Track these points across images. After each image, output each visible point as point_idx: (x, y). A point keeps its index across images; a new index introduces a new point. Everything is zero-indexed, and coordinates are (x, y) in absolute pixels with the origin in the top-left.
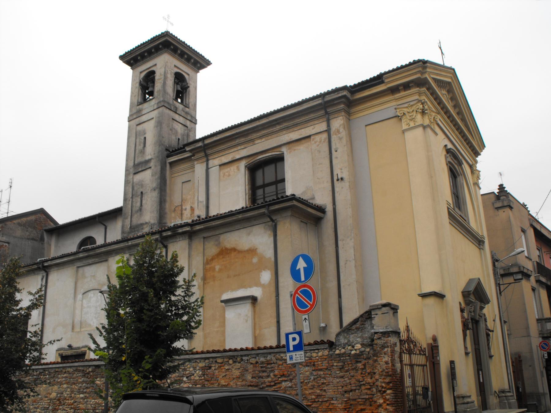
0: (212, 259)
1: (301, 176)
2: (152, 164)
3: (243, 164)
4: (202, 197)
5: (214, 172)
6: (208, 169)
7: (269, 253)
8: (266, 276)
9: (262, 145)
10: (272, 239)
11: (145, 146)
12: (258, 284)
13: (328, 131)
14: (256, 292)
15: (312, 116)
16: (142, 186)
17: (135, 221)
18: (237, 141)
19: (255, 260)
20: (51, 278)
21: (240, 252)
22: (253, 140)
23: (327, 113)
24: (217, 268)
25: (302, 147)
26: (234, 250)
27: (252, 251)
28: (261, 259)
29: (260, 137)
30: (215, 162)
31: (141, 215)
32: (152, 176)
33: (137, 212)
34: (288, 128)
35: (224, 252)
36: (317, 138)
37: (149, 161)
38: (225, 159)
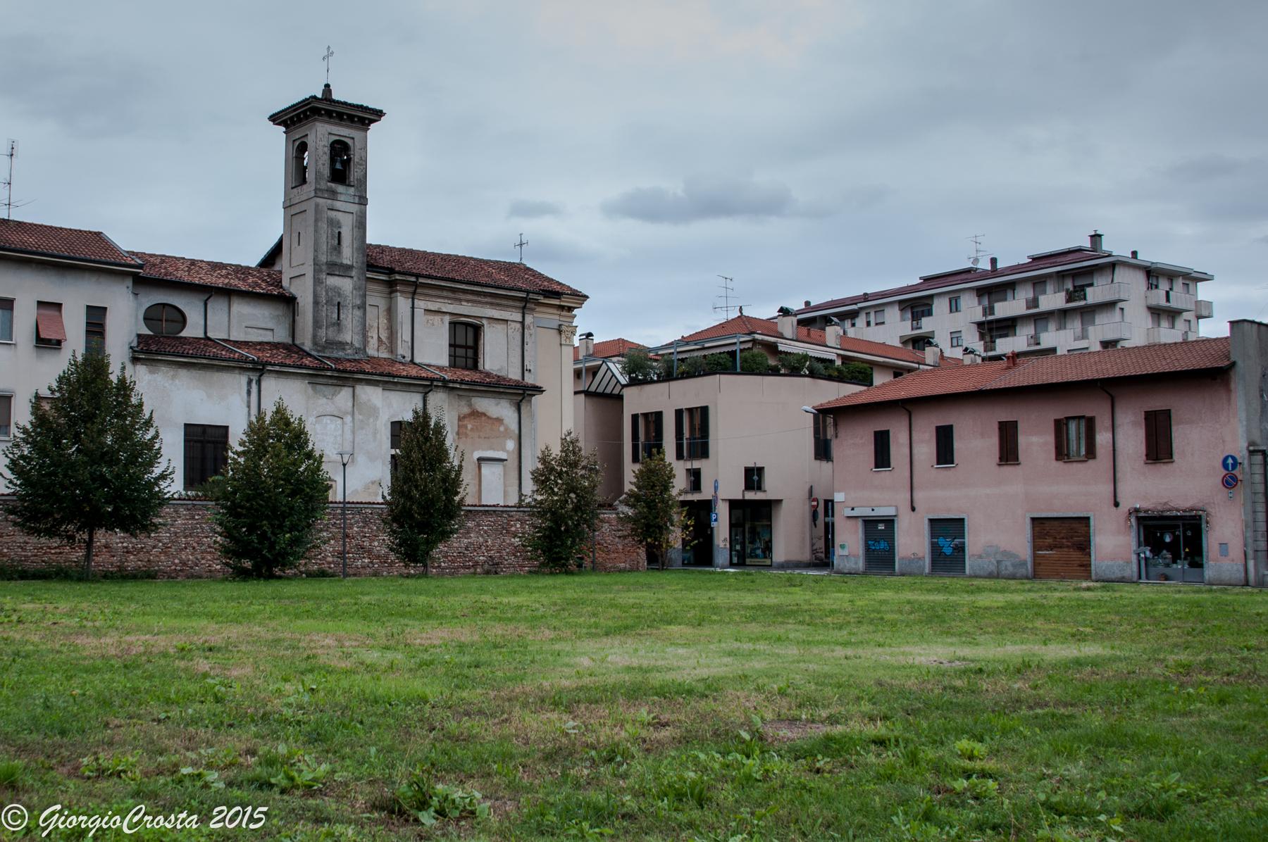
0: (464, 417)
1: (497, 355)
2: (353, 274)
3: (447, 319)
4: (407, 337)
5: (419, 313)
6: (413, 308)
7: (514, 427)
8: (511, 445)
9: (468, 309)
10: (516, 415)
11: (339, 243)
12: (504, 449)
13: (523, 323)
14: (502, 455)
15: (511, 303)
16: (339, 295)
17: (332, 333)
18: (445, 294)
19: (502, 429)
20: (263, 384)
21: (489, 418)
22: (460, 300)
23: (524, 308)
24: (469, 427)
25: (500, 327)
26: (484, 414)
27: (499, 420)
28: (507, 429)
29: (468, 301)
30: (421, 304)
31: (340, 331)
32: (354, 288)
33: (334, 324)
34: (492, 304)
35: (475, 414)
36: (513, 325)
37: (350, 267)
38: (433, 306)
